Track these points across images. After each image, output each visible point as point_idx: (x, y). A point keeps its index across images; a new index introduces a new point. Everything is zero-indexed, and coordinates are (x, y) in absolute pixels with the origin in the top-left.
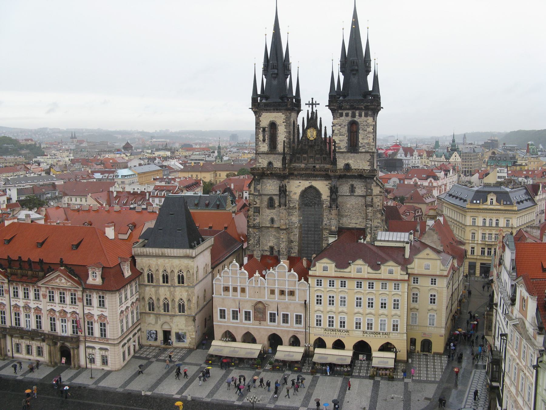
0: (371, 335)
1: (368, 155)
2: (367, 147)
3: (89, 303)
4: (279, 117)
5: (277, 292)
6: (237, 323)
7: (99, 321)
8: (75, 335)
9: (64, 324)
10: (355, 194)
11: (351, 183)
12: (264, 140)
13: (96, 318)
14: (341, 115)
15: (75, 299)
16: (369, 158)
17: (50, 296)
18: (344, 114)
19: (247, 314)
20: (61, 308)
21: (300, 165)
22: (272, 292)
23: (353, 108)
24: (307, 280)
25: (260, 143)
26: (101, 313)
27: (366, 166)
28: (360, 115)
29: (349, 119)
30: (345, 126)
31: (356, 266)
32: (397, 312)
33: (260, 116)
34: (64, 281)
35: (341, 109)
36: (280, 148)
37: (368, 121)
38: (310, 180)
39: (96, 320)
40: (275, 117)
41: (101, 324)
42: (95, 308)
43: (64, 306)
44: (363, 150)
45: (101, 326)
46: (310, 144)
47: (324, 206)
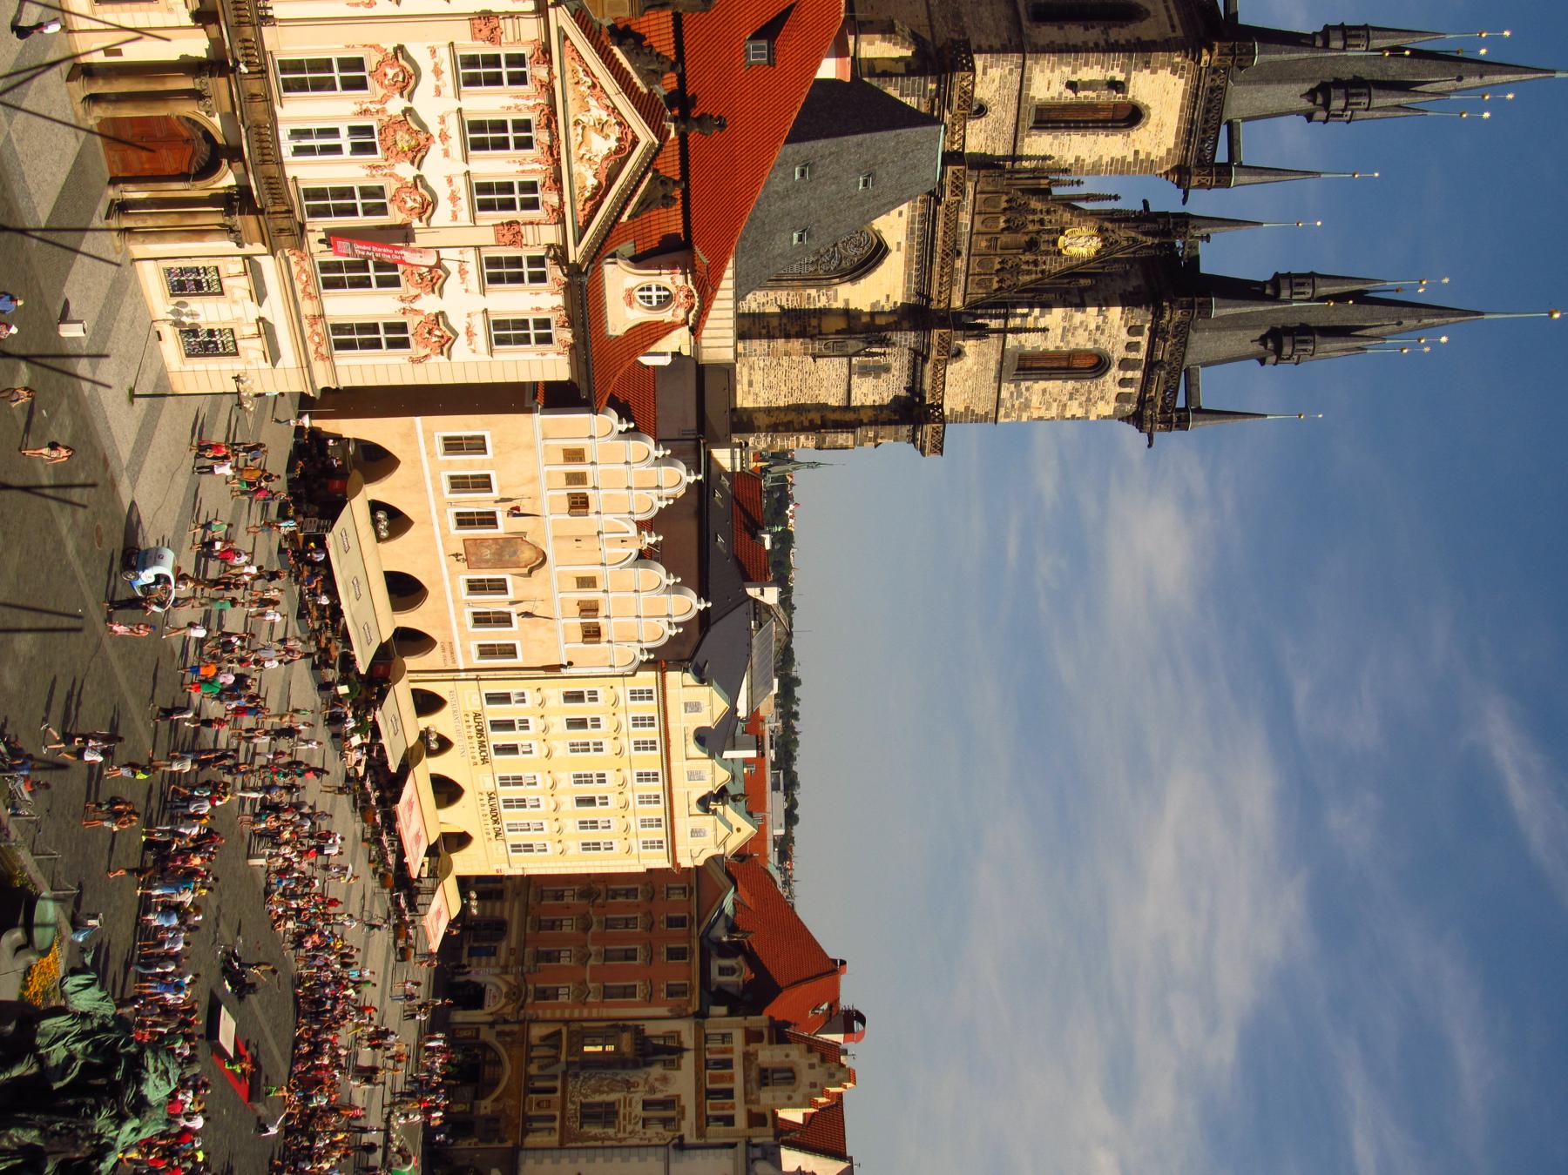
0: (487, 809)
1: (990, 406)
2: (1017, 403)
3: (500, 272)
4: (1159, 137)
5: (588, 595)
6: (437, 490)
7: (412, 322)
8: (300, 206)
9: (345, 141)
10: (855, 378)
11: (896, 365)
12: (1072, 86)
13: (429, 304)
14: (1133, 330)
15: (510, 205)
16: (980, 411)
17: (494, 60)
18: (1135, 339)
19: (489, 520)
20: (434, 129)
21: (969, 208)
22: (586, 582)
23: (1151, 365)
24: (644, 666)
25: (1067, 70)
26: (461, 330)
27: (953, 401)
28: (1123, 382)
29: (1119, 353)
30: (1096, 341)
31: (709, 771)
32: (574, 847)
33: (1174, 72)
34: (602, 146)
35: (1154, 332)
36: (1039, 144)
37: (1101, 404)
38: (911, 247)
39: (417, 305)
40: (1161, 125)
41: (403, 327)
42: (479, 303)
43: (455, 143)
44: (1004, 394)
45: (390, 328)
46: (1046, 237)
47: (813, 292)
